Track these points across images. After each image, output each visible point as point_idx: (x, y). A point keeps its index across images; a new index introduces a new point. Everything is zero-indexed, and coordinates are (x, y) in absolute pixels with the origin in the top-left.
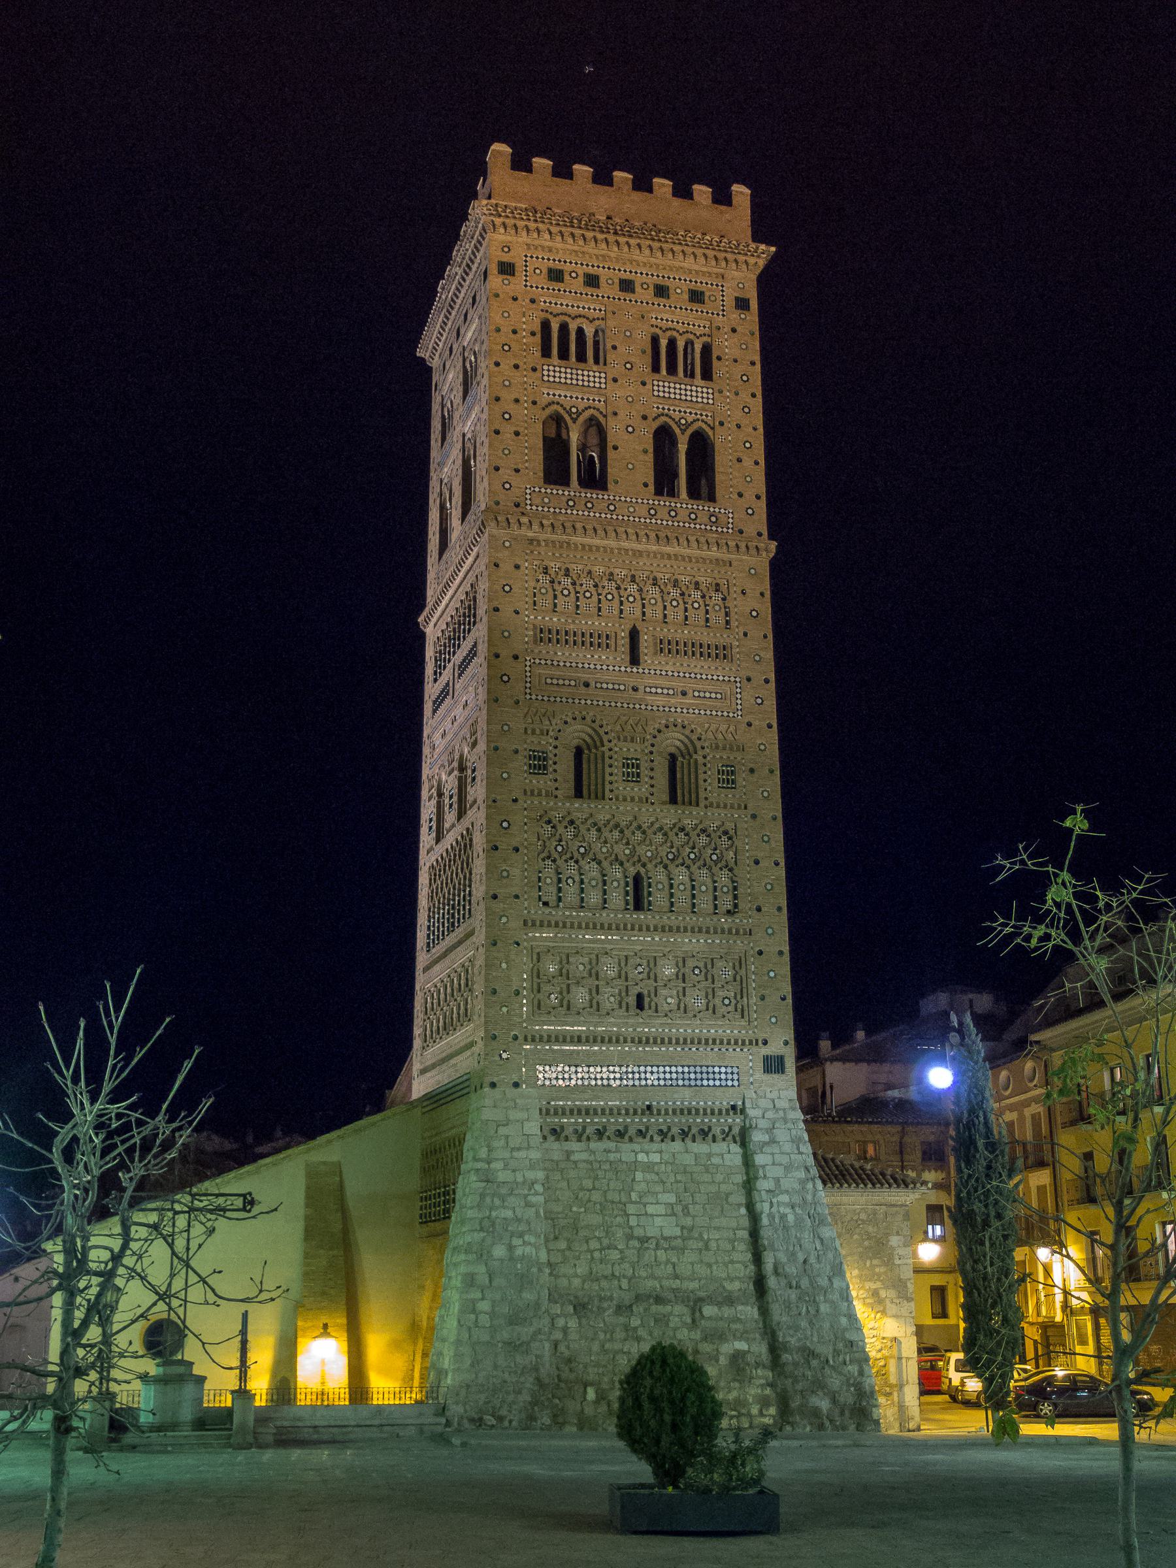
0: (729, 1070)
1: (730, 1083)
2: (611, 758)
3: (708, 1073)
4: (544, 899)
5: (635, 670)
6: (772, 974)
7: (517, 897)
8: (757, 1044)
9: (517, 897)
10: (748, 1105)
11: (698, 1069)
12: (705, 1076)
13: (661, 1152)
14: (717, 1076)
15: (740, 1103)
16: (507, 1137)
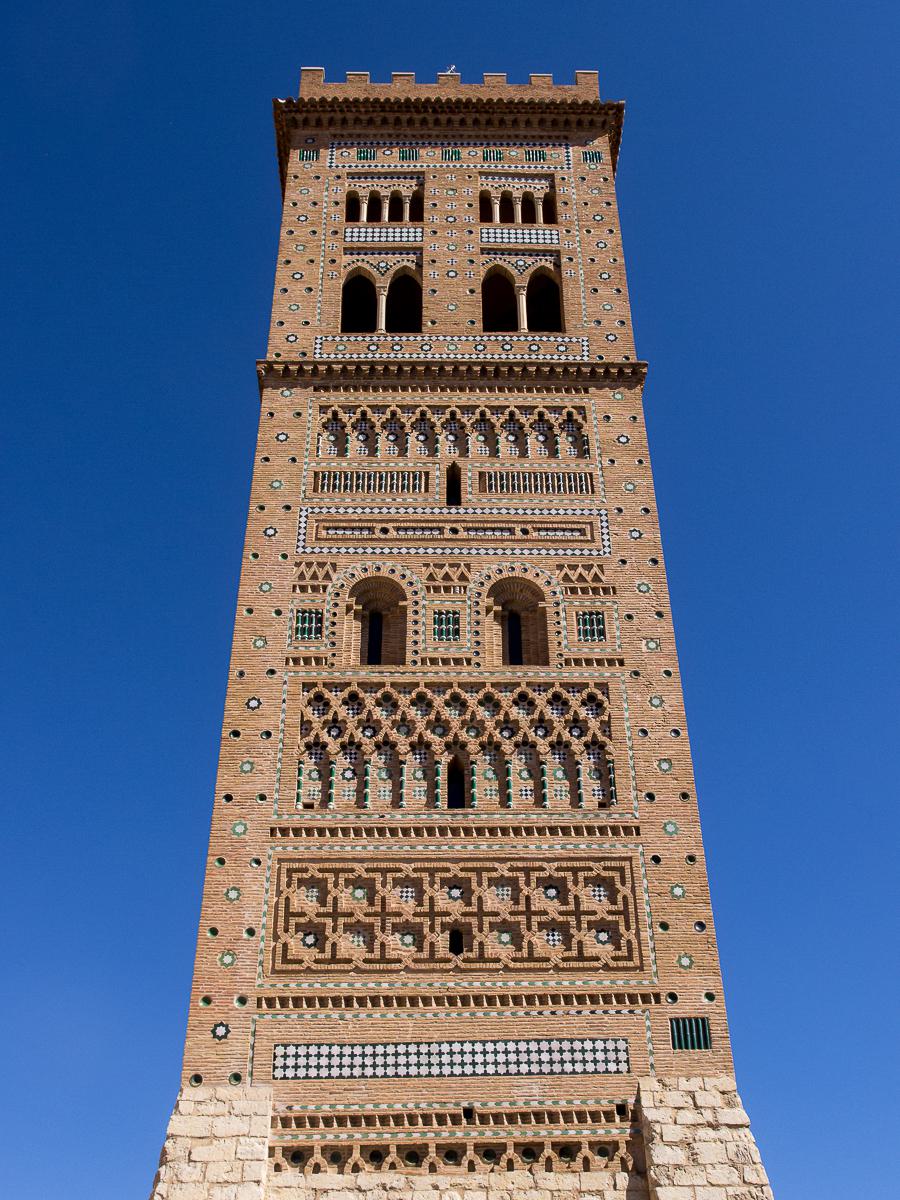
0: (611, 1045)
1: (612, 1067)
2: (416, 612)
3: (572, 1051)
4: (305, 800)
5: (453, 511)
6: (678, 891)
7: (263, 797)
8: (658, 1001)
9: (263, 797)
10: (646, 1101)
11: (555, 1045)
12: (567, 1056)
13: (486, 1189)
14: (589, 1056)
15: (631, 1101)
16: (206, 1163)
